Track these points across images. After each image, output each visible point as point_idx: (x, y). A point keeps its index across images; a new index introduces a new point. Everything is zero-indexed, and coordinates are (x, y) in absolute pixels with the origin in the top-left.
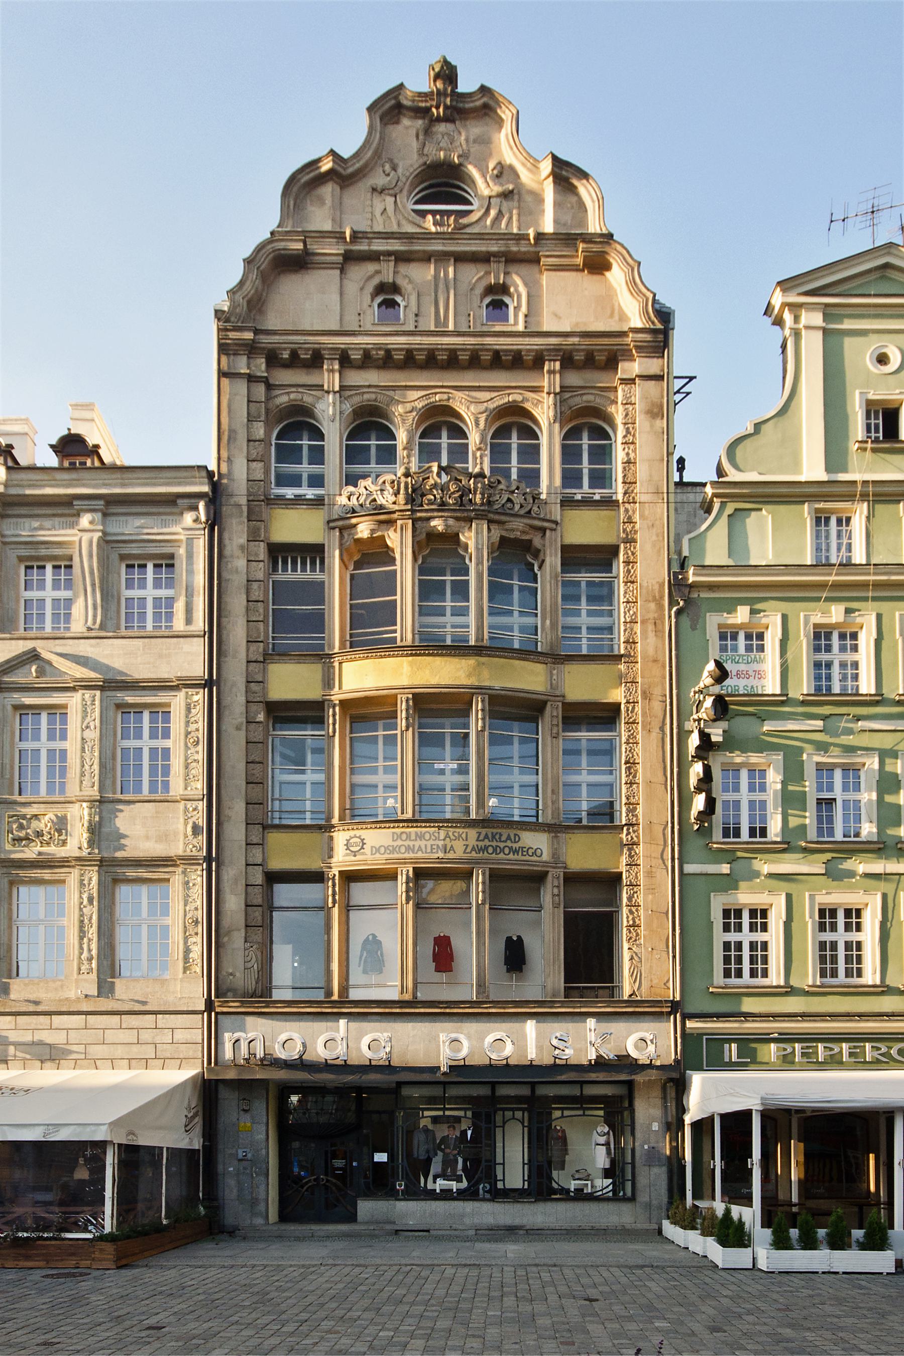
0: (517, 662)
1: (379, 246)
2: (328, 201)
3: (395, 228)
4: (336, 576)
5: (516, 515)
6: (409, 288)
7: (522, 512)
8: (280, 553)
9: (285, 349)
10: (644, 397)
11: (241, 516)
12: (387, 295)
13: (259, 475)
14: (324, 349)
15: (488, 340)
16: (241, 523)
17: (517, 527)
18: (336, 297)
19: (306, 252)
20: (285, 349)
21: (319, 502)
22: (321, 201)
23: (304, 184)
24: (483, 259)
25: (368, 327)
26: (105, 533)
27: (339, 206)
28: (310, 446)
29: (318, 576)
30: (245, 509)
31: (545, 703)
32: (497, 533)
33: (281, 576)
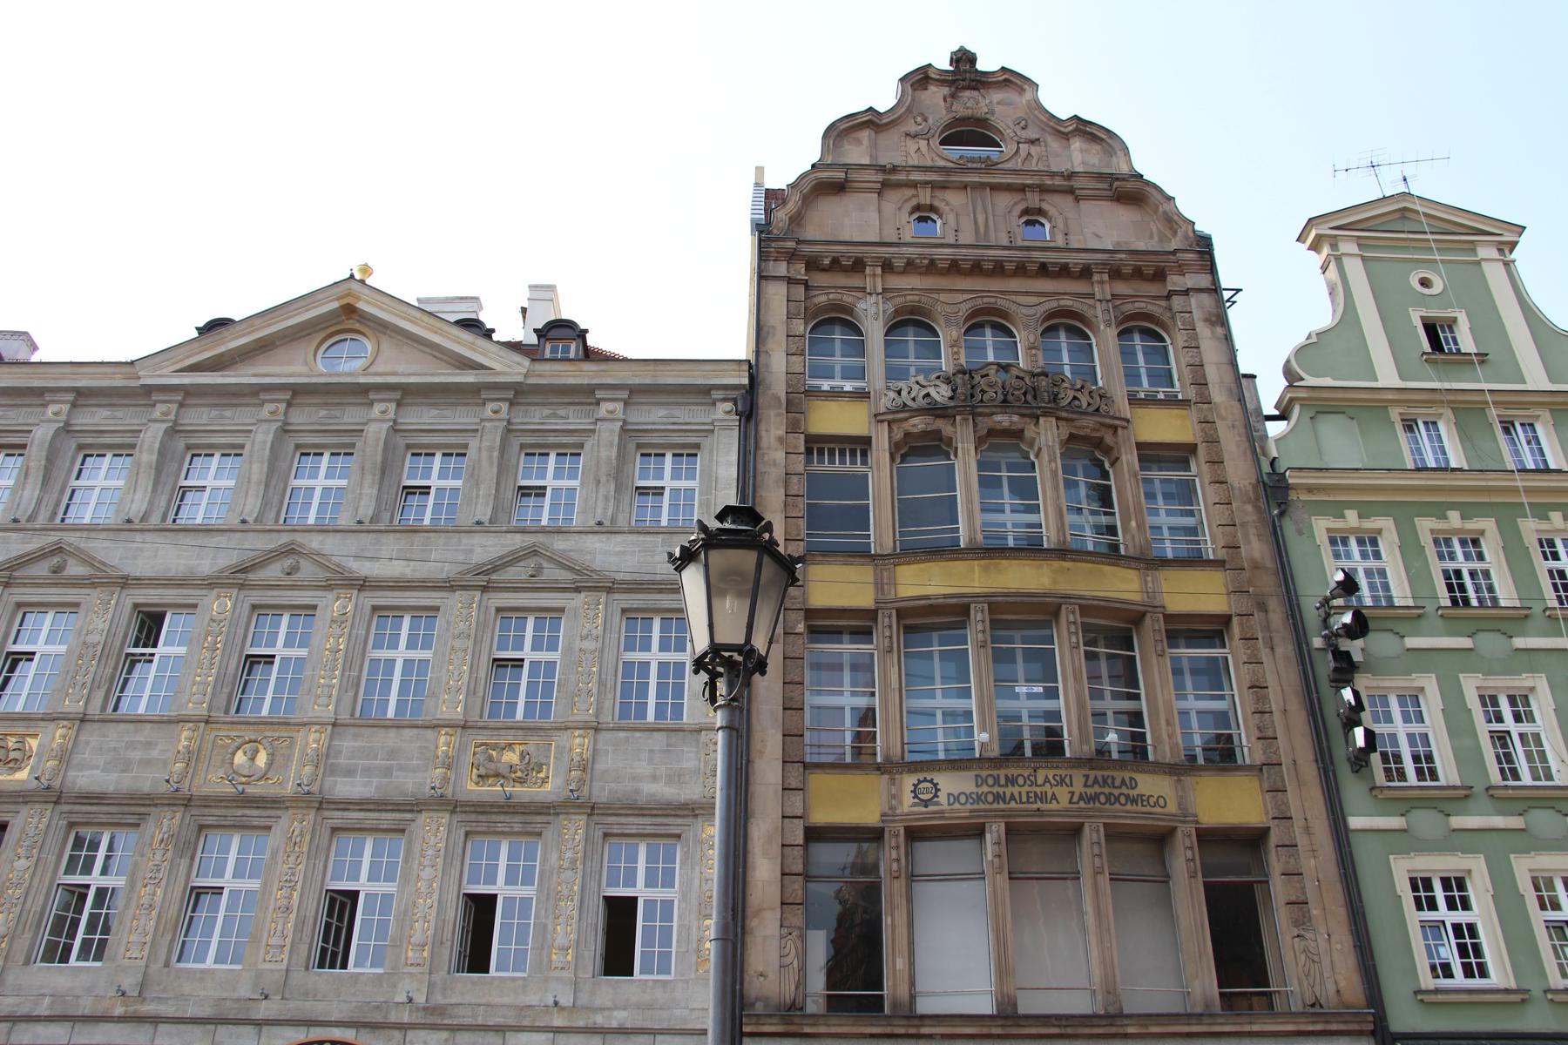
0: (1106, 568)
1: (915, 176)
2: (865, 142)
3: (929, 163)
4: (879, 473)
5: (1085, 413)
6: (947, 209)
7: (1091, 409)
8: (817, 445)
10: (1201, 307)
12: (924, 214)
13: (799, 369)
15: (1035, 254)
17: (1087, 424)
18: (875, 215)
19: (846, 180)
21: (861, 395)
22: (859, 142)
23: (841, 131)
24: (1022, 189)
25: (908, 239)
26: (625, 422)
27: (874, 146)
29: (859, 468)
31: (1143, 614)
32: (1065, 434)
33: (816, 467)
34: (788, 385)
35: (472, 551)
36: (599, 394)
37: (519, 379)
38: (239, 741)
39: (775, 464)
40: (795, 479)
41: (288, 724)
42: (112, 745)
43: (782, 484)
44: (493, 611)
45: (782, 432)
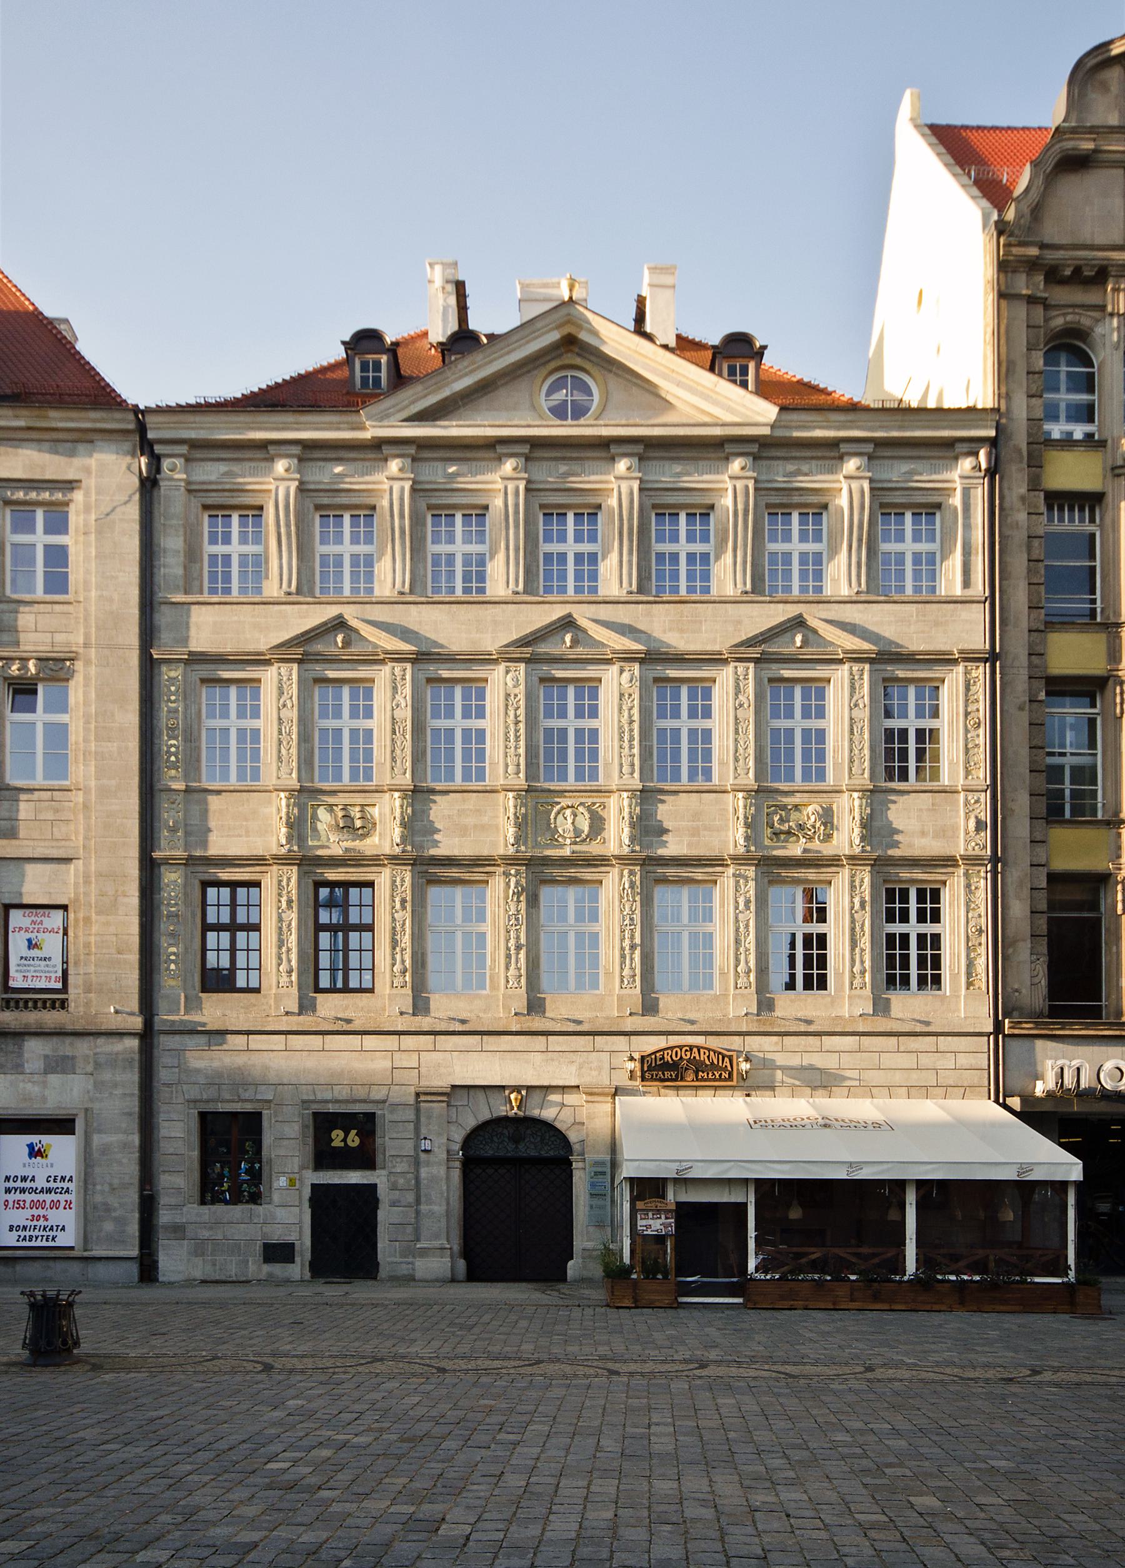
9: (1069, 266)
11: (1021, 462)
14: (1113, 266)
16: (1021, 470)
20: (1069, 266)
28: (1068, 372)
30: (1025, 454)
34: (1029, 435)
35: (739, 622)
36: (844, 448)
37: (766, 431)
38: (558, 807)
39: (1018, 525)
40: (1036, 543)
41: (600, 791)
42: (446, 812)
43: (1024, 549)
44: (766, 680)
45: (1023, 490)
